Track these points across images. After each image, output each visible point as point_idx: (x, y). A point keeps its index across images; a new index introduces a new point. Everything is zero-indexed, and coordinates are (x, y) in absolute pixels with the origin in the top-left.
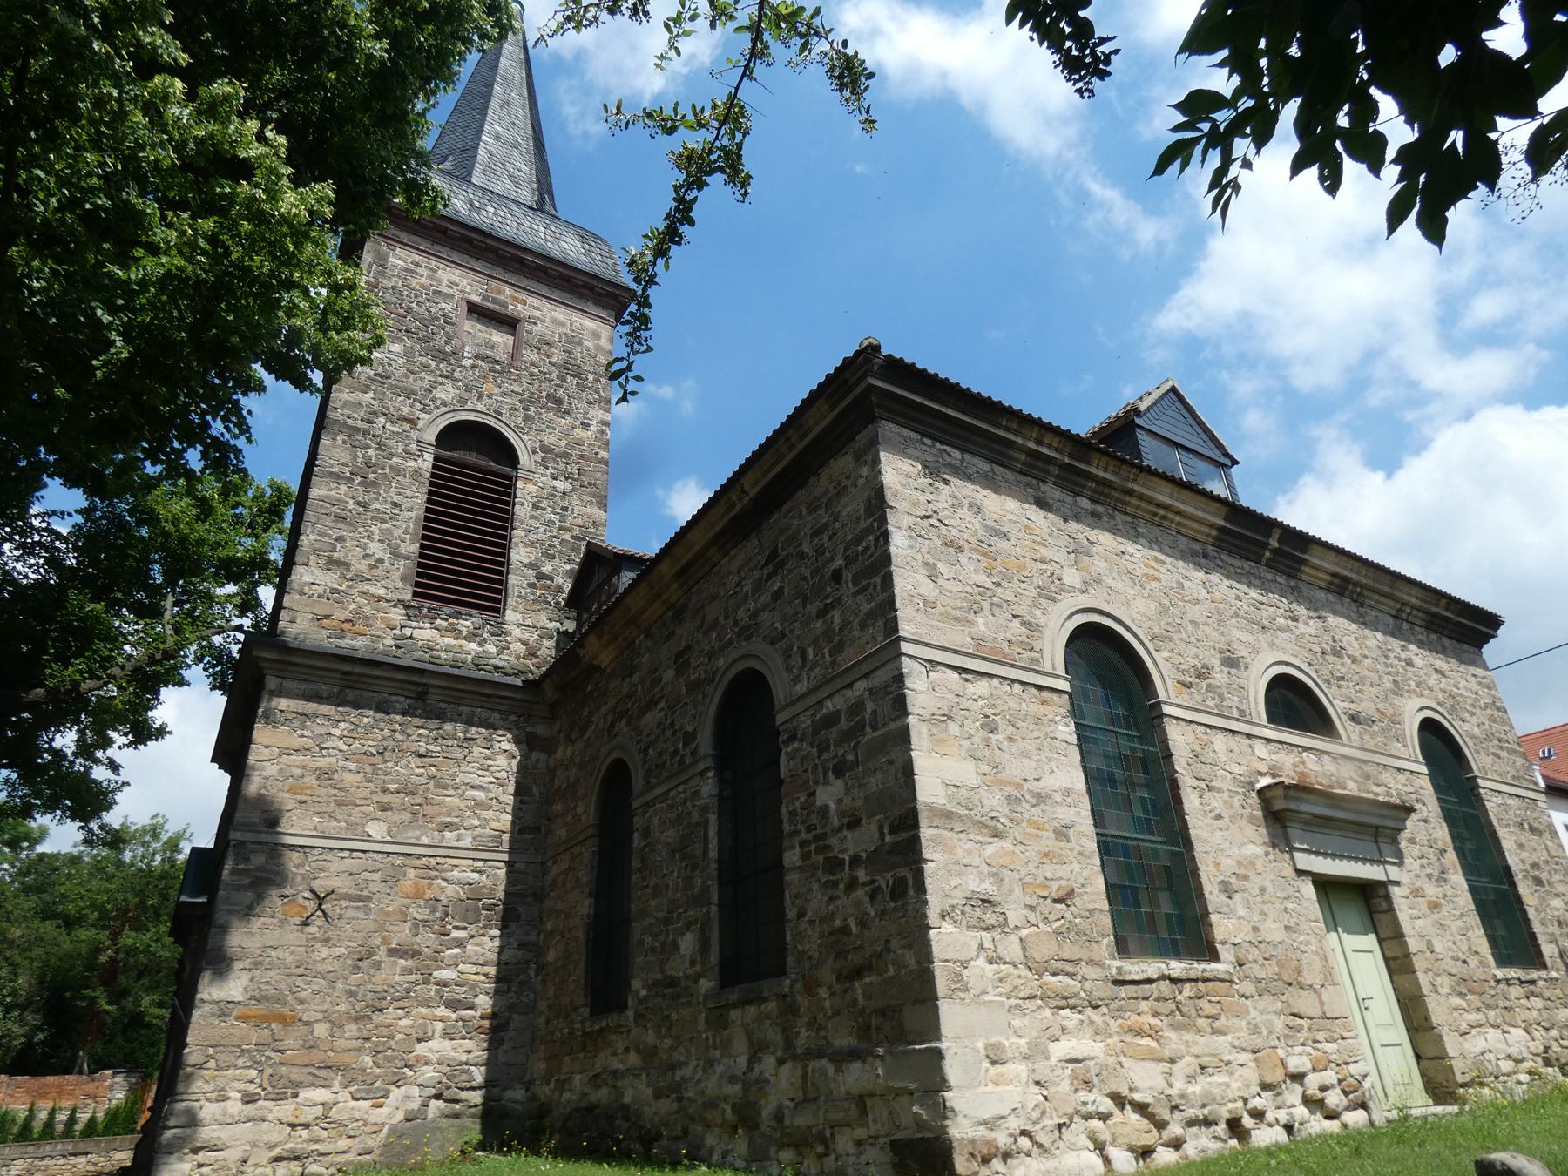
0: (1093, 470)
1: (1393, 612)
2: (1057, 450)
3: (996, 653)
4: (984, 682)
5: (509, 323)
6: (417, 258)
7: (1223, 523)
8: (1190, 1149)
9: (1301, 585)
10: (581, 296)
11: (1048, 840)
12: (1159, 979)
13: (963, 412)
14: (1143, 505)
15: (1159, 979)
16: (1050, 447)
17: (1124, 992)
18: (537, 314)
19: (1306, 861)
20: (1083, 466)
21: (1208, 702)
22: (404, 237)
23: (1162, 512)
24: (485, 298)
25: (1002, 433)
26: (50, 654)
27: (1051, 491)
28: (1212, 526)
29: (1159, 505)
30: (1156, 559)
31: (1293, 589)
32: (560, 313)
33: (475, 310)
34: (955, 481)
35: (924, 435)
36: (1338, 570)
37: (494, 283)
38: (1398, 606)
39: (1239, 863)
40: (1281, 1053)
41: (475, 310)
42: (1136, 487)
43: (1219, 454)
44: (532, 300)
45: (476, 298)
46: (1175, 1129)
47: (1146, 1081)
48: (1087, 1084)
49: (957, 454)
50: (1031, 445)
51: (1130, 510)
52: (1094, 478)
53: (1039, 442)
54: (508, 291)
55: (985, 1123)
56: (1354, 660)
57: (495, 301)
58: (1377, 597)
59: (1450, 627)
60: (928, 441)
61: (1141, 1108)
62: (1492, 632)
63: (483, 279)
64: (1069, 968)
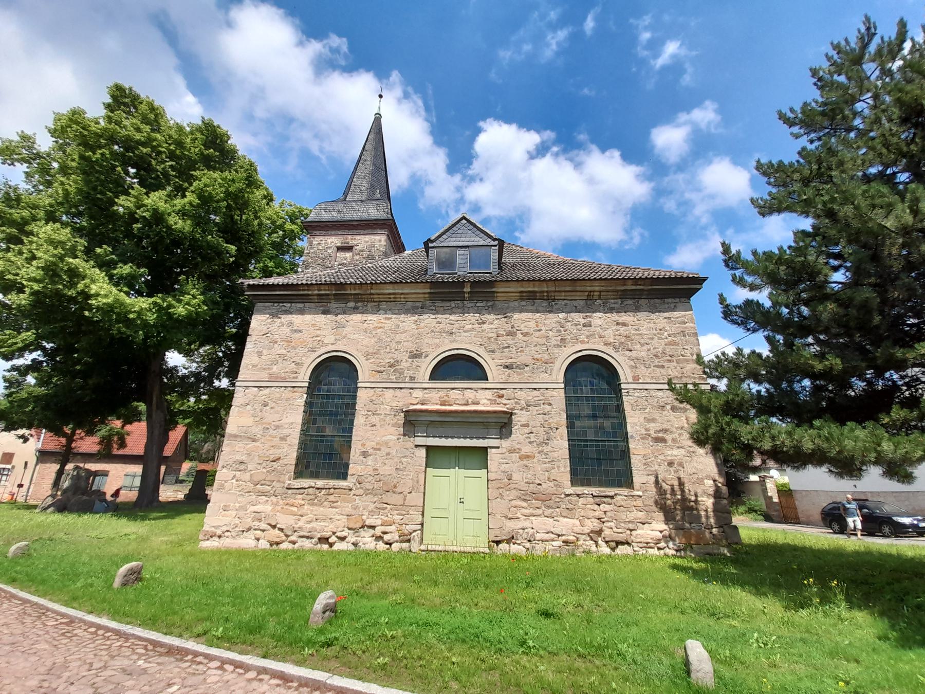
0: (348, 292)
1: (586, 298)
2: (329, 290)
3: (277, 377)
4: (268, 389)
5: (349, 249)
6: (321, 238)
7: (429, 291)
8: (335, 548)
9: (496, 302)
10: (375, 229)
11: (276, 441)
12: (309, 488)
13: (280, 291)
14: (381, 296)
15: (309, 488)
16: (325, 290)
17: (290, 492)
18: (359, 241)
19: (420, 441)
20: (343, 292)
21: (391, 377)
22: (318, 233)
23: (392, 296)
24: (342, 243)
25: (302, 293)
26: (177, 401)
27: (333, 305)
28: (424, 293)
29: (390, 294)
30: (386, 318)
31: (492, 306)
32: (367, 238)
33: (339, 249)
34: (283, 316)
35: (274, 303)
36: (522, 289)
37: (345, 237)
38: (587, 294)
39: (377, 444)
40: (364, 517)
41: (339, 249)
42: (372, 291)
43: (489, 240)
44: (358, 237)
45: (339, 245)
46: (293, 538)
47: (285, 521)
48: (260, 520)
49: (289, 305)
50: (316, 292)
51: (376, 300)
52: (351, 294)
53: (319, 290)
54: (350, 237)
55: (214, 527)
56: (525, 334)
57: (345, 243)
58: (563, 294)
59: (645, 293)
60: (276, 305)
61: (281, 530)
62: (697, 286)
63: (341, 237)
64: (268, 483)
